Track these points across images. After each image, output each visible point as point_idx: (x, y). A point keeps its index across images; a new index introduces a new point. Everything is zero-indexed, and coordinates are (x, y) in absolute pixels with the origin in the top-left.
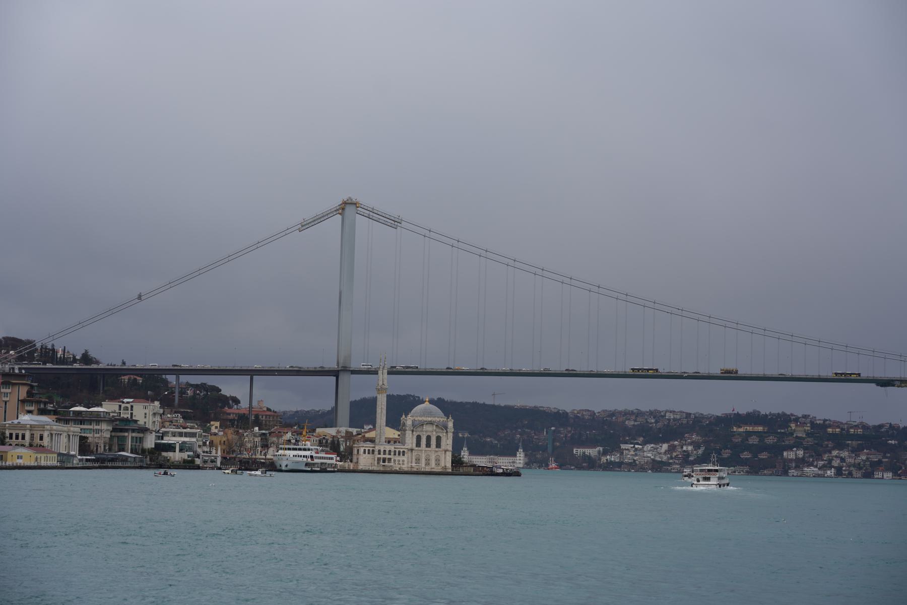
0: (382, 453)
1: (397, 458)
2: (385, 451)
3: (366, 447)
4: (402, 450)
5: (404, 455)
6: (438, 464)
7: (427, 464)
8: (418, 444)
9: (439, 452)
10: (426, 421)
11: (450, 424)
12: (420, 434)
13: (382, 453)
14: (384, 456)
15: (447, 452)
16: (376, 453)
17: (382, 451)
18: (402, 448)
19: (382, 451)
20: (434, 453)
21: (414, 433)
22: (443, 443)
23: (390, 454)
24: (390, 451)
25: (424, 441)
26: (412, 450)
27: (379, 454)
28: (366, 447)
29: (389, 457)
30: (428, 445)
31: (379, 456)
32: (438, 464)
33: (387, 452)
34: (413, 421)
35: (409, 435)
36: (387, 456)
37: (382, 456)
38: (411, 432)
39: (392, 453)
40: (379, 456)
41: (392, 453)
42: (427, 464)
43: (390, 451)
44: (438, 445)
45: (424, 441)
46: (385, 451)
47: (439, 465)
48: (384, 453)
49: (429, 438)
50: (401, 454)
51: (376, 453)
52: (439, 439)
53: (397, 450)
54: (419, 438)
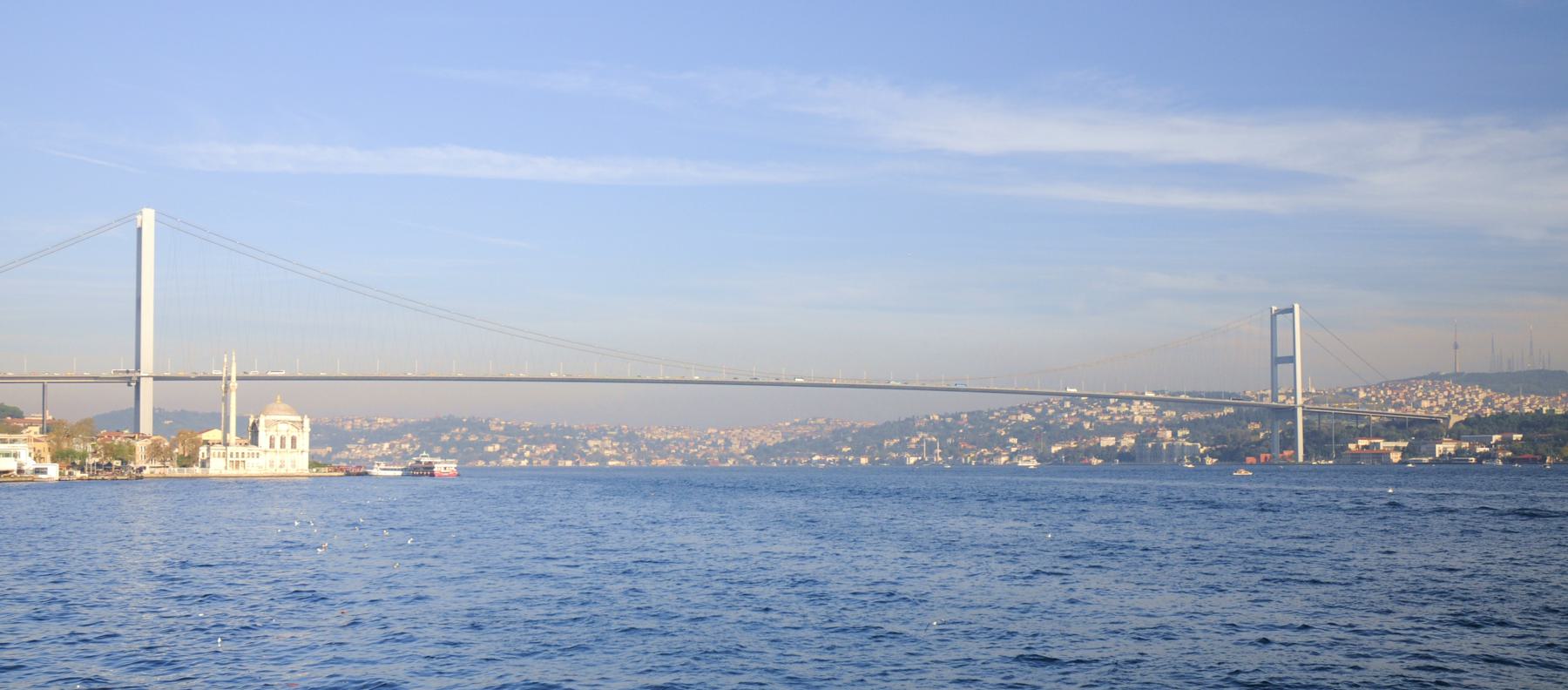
2: (237, 453)
6: (294, 466)
8: (272, 446)
11: (307, 422)
13: (234, 456)
16: (229, 456)
17: (234, 454)
19: (234, 454)
22: (298, 444)
25: (277, 443)
26: (266, 451)
27: (231, 456)
29: (243, 459)
30: (283, 445)
31: (232, 459)
33: (240, 455)
34: (266, 421)
36: (240, 459)
37: (234, 459)
45: (277, 443)
49: (283, 439)
50: (255, 457)
52: (294, 440)
54: (272, 439)
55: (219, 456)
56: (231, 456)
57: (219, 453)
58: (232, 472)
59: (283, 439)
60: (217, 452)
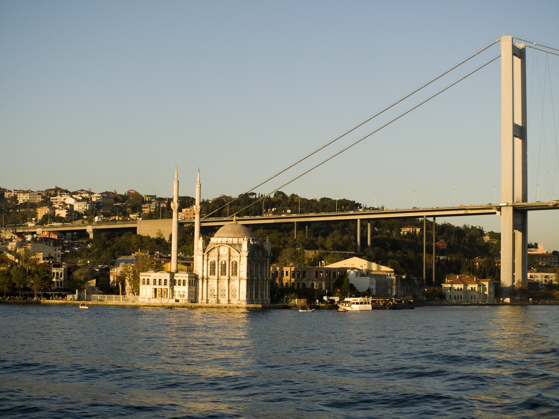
0: (157, 283)
3: (144, 276)
5: (184, 285)
8: (213, 272)
13: (157, 283)
17: (157, 281)
19: (157, 281)
21: (206, 258)
23: (165, 284)
27: (155, 284)
28: (144, 276)
30: (224, 272)
31: (155, 287)
36: (163, 287)
37: (157, 287)
40: (155, 287)
41: (168, 283)
43: (165, 280)
50: (182, 284)
51: (151, 282)
52: (235, 265)
55: (148, 284)
56: (155, 284)
57: (148, 280)
58: (157, 301)
59: (224, 267)
60: (146, 278)
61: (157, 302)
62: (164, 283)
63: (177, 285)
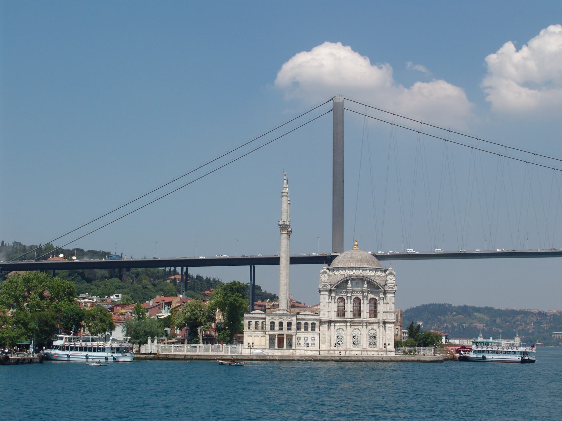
0: (277, 327)
1: (302, 334)
2: (281, 324)
4: (310, 323)
5: (313, 329)
7: (357, 343)
9: (374, 325)
10: (352, 276)
12: (343, 295)
13: (277, 327)
14: (280, 333)
15: (387, 325)
18: (310, 320)
20: (367, 326)
21: (333, 294)
22: (381, 308)
23: (289, 328)
24: (289, 324)
26: (330, 322)
27: (272, 328)
30: (357, 313)
31: (272, 333)
32: (372, 343)
33: (285, 325)
35: (324, 298)
36: (285, 332)
37: (277, 332)
38: (327, 293)
39: (294, 327)
41: (294, 327)
42: (357, 343)
43: (289, 324)
44: (374, 313)
46: (281, 324)
47: (375, 344)
48: (281, 328)
50: (310, 329)
51: (268, 327)
53: (303, 322)
56: (272, 328)
61: (276, 354)
62: (286, 326)
63: (303, 330)
